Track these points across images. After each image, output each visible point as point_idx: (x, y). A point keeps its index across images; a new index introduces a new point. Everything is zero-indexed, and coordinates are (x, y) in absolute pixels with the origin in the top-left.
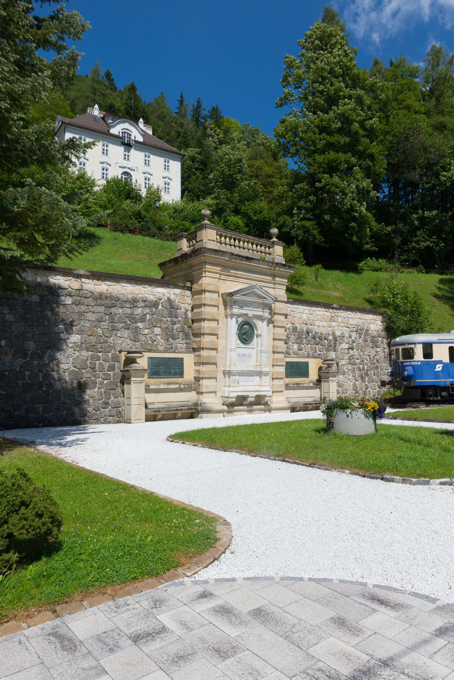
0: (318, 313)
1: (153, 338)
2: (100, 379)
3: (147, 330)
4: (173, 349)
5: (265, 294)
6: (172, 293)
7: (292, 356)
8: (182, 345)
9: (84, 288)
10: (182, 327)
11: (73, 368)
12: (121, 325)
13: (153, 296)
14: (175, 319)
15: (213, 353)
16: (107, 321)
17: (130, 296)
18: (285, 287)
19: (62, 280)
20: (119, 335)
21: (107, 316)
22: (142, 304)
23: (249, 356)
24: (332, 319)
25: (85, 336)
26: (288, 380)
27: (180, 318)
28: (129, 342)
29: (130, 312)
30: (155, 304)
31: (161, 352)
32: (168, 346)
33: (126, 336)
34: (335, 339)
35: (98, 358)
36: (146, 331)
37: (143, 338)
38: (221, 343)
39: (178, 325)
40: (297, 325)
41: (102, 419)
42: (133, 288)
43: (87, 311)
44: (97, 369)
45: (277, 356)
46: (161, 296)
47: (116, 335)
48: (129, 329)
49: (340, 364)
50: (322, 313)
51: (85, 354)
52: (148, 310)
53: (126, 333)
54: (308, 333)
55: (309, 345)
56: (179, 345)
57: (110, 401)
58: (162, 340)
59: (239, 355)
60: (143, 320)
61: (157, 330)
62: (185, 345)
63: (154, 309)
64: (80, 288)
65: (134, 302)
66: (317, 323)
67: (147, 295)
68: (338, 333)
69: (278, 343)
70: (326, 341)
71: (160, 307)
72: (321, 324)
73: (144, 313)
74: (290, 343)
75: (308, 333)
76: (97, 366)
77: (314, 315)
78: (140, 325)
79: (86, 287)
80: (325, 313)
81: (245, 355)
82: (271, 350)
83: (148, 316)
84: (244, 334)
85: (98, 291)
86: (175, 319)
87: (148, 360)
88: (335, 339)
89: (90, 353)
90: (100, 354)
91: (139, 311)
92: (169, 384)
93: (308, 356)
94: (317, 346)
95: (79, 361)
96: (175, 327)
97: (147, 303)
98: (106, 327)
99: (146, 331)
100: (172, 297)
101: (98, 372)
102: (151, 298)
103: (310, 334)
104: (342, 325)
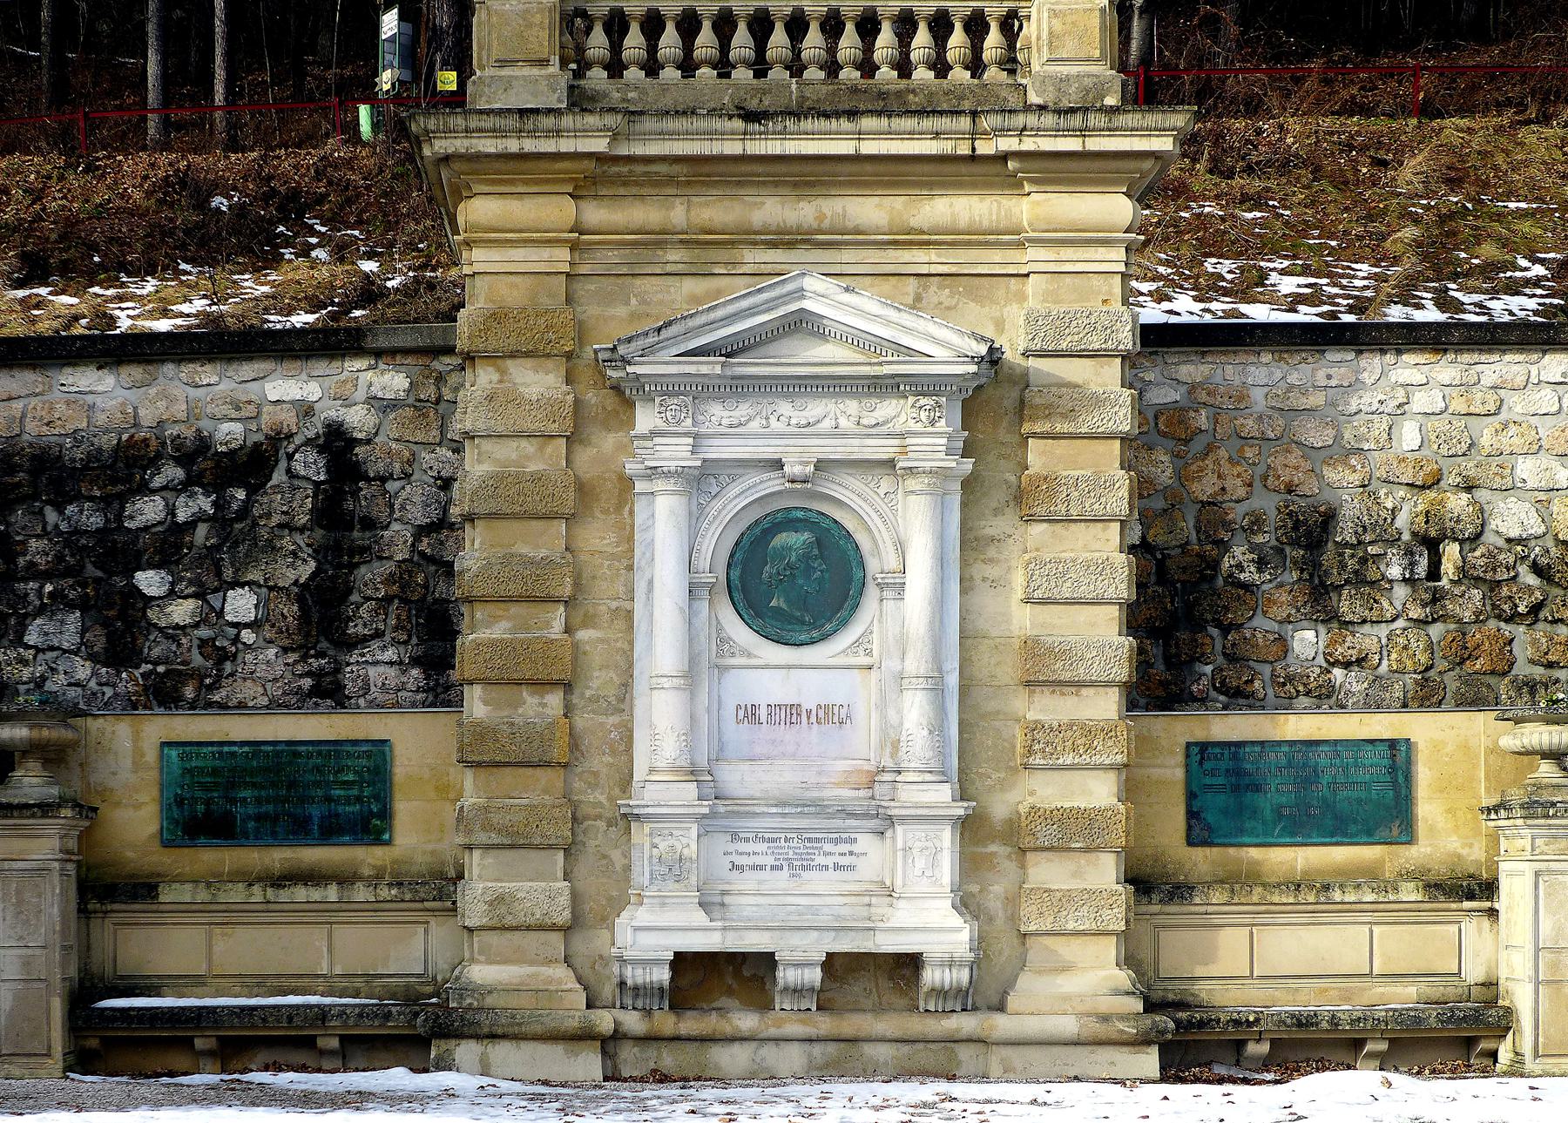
12: (49, 588)
13: (237, 428)
22: (172, 473)
23: (831, 716)
28: (83, 670)
31: (256, 711)
33: (69, 639)
36: (182, 611)
42: (131, 395)
46: (288, 419)
59: (750, 714)
65: (127, 464)
71: (279, 477)
73: (182, 516)
78: (150, 581)
81: (791, 713)
83: (202, 530)
91: (148, 510)
93: (1426, 696)
99: (182, 611)
102: (229, 433)
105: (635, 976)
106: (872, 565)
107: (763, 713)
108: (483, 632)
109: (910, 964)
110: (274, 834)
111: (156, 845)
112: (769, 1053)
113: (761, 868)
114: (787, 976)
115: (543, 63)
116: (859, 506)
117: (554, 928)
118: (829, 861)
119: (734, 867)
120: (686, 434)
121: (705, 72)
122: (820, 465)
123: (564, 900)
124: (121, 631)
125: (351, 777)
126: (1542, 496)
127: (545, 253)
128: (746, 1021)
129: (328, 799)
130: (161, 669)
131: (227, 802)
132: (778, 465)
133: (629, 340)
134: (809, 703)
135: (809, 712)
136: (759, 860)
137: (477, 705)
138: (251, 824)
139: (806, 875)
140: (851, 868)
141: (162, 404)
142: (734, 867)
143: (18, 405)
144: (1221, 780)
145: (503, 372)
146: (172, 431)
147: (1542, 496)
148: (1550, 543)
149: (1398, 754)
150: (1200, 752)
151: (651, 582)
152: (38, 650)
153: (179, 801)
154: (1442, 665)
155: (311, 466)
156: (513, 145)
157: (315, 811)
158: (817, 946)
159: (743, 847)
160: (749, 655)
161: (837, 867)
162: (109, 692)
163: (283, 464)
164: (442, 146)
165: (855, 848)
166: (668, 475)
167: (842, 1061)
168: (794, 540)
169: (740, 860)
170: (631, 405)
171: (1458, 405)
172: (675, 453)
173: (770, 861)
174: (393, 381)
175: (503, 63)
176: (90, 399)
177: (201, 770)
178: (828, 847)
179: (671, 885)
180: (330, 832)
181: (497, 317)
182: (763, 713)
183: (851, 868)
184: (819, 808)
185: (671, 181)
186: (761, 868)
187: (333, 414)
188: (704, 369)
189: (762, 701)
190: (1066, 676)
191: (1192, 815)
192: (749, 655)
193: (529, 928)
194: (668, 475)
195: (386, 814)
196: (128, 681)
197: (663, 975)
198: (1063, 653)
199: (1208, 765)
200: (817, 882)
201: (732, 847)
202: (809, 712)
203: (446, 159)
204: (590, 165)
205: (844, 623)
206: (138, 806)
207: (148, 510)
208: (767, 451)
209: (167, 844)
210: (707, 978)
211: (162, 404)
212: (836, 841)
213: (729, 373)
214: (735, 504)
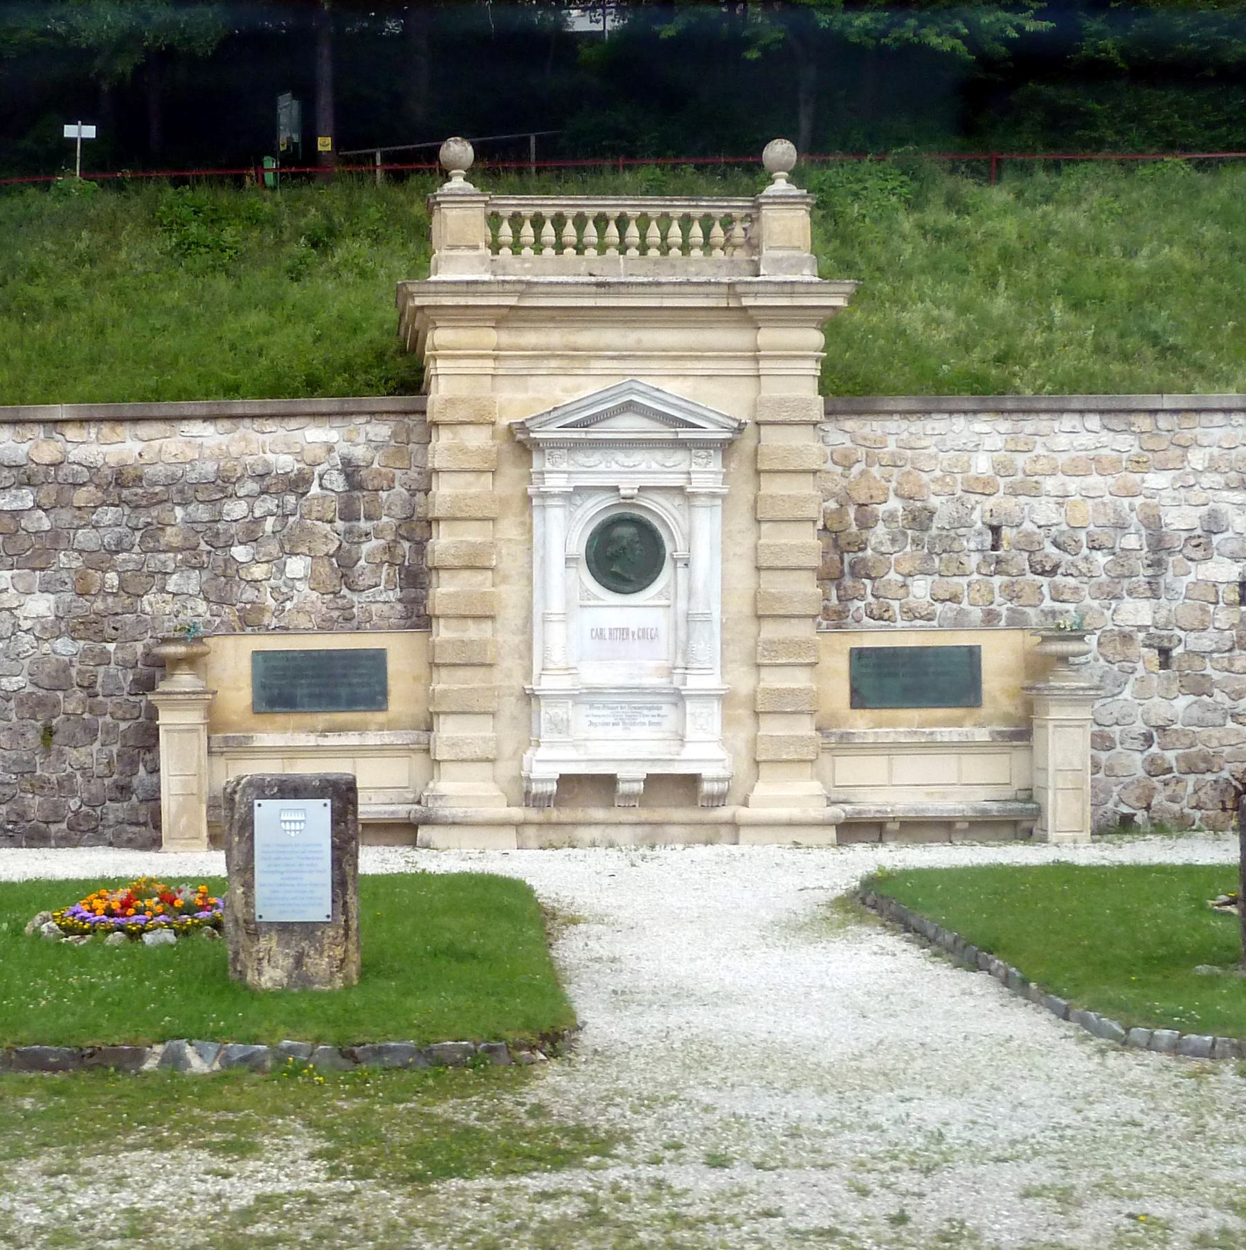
0: (1062, 441)
1: (284, 590)
2: (108, 718)
3: (265, 566)
4: (355, 623)
5: (681, 409)
6: (362, 439)
7: (900, 624)
8: (386, 608)
9: (72, 459)
10: (389, 549)
11: (30, 689)
12: (180, 557)
13: (290, 458)
14: (364, 525)
15: (473, 631)
16: (137, 549)
17: (210, 468)
18: (812, 368)
19: (11, 443)
20: (170, 588)
21: (138, 534)
22: (251, 487)
23: (646, 635)
24: (1139, 464)
25: (68, 597)
26: (863, 723)
27: (385, 519)
28: (202, 607)
29: (206, 517)
30: (297, 483)
31: (307, 631)
32: (335, 614)
33: (193, 588)
34: (1159, 545)
35: (104, 658)
36: (258, 571)
37: (250, 594)
38: (509, 595)
39: (374, 543)
40: (934, 502)
41: (109, 833)
42: (225, 439)
43: (76, 522)
44: (98, 689)
45: (771, 631)
47: (163, 590)
48: (201, 568)
49: (1174, 653)
50: (1084, 439)
51: (65, 647)
52: (270, 503)
53: (193, 582)
54: (995, 530)
55: (997, 580)
56: (374, 607)
57: (135, 781)
58: (315, 594)
59: (599, 634)
60: (251, 536)
61: (297, 566)
62: (399, 607)
63: (291, 499)
64: (59, 457)
66: (1050, 484)
67: (270, 457)
68: (1180, 519)
69: (775, 584)
70: (1101, 558)
71: (315, 489)
72: (1073, 485)
73: (257, 514)
74: (892, 575)
75: (995, 530)
76: (100, 680)
77: (1040, 450)
79: (76, 454)
80: (1106, 437)
81: (624, 633)
82: (747, 610)
83: (271, 520)
84: (613, 558)
85: (112, 461)
86: (364, 525)
87: (254, 661)
88: (1159, 545)
89: (82, 643)
90: (111, 647)
91: (237, 509)
92: (324, 732)
93: (990, 618)
94: (1044, 580)
95: (48, 668)
96: (366, 548)
97: (268, 481)
98: (131, 566)
100: (360, 453)
101: (100, 698)
102: (285, 463)
103: (1006, 532)
104: (1208, 480)
105: (536, 788)
106: (669, 548)
107: (607, 633)
108: (445, 591)
109: (692, 781)
110: (320, 705)
111: (249, 714)
112: (612, 833)
113: (607, 724)
114: (623, 788)
115: (476, 248)
116: (663, 511)
117: (488, 760)
118: (646, 720)
119: (591, 723)
120: (564, 472)
121: (570, 251)
122: (641, 489)
123: (492, 744)
124: (223, 583)
125: (364, 671)
126: (1061, 500)
127: (480, 363)
128: (599, 814)
129: (350, 685)
130: (248, 606)
131: (294, 685)
132: (617, 489)
133: (532, 419)
134: (633, 628)
135: (633, 633)
136: (606, 720)
137: (444, 632)
138: (306, 700)
139: (632, 728)
140: (658, 724)
141: (243, 444)
142: (591, 723)
143: (156, 444)
144: (869, 670)
145: (455, 434)
146: (249, 460)
147: (1061, 500)
148: (1064, 527)
149: (973, 654)
150: (859, 656)
151: (543, 558)
152: (175, 595)
153: (264, 686)
154: (999, 600)
155: (338, 482)
156: (462, 301)
157: (344, 692)
158: (641, 772)
159: (596, 712)
160: (599, 599)
161: (651, 724)
162: (218, 620)
163: (316, 482)
164: (419, 302)
165: (662, 712)
166: (553, 496)
167: (652, 835)
168: (627, 531)
169: (594, 720)
170: (529, 452)
171: (1012, 446)
172: (556, 483)
173: (612, 720)
174: (381, 430)
175: (452, 247)
176: (199, 440)
177: (274, 668)
178: (645, 712)
179: (556, 735)
180: (352, 703)
181: (450, 402)
182: (607, 633)
183: (658, 724)
184: (641, 691)
185: (552, 319)
186: (607, 724)
187: (345, 451)
188: (576, 436)
189: (606, 626)
190: (781, 612)
191: (854, 691)
192: (599, 599)
193: (472, 761)
194: (553, 496)
195: (384, 693)
196: (229, 614)
197: (552, 788)
198: (777, 598)
199: (864, 661)
200: (637, 732)
201: (590, 712)
202: (633, 633)
203: (422, 308)
204: (505, 311)
205: (653, 580)
206: (239, 689)
207: (237, 509)
208: (610, 482)
209: (256, 713)
210: (573, 786)
211: (243, 444)
212: (650, 709)
213: (590, 436)
214: (592, 511)
